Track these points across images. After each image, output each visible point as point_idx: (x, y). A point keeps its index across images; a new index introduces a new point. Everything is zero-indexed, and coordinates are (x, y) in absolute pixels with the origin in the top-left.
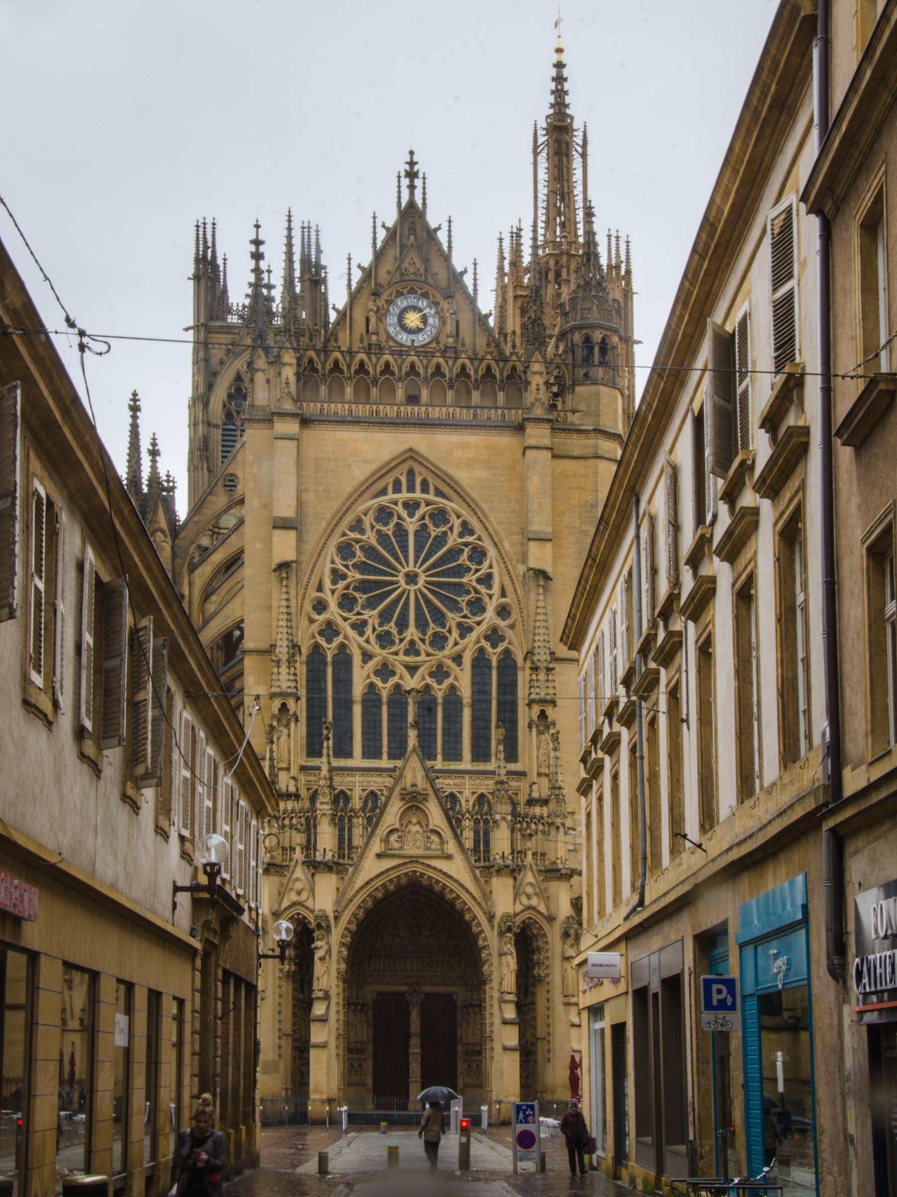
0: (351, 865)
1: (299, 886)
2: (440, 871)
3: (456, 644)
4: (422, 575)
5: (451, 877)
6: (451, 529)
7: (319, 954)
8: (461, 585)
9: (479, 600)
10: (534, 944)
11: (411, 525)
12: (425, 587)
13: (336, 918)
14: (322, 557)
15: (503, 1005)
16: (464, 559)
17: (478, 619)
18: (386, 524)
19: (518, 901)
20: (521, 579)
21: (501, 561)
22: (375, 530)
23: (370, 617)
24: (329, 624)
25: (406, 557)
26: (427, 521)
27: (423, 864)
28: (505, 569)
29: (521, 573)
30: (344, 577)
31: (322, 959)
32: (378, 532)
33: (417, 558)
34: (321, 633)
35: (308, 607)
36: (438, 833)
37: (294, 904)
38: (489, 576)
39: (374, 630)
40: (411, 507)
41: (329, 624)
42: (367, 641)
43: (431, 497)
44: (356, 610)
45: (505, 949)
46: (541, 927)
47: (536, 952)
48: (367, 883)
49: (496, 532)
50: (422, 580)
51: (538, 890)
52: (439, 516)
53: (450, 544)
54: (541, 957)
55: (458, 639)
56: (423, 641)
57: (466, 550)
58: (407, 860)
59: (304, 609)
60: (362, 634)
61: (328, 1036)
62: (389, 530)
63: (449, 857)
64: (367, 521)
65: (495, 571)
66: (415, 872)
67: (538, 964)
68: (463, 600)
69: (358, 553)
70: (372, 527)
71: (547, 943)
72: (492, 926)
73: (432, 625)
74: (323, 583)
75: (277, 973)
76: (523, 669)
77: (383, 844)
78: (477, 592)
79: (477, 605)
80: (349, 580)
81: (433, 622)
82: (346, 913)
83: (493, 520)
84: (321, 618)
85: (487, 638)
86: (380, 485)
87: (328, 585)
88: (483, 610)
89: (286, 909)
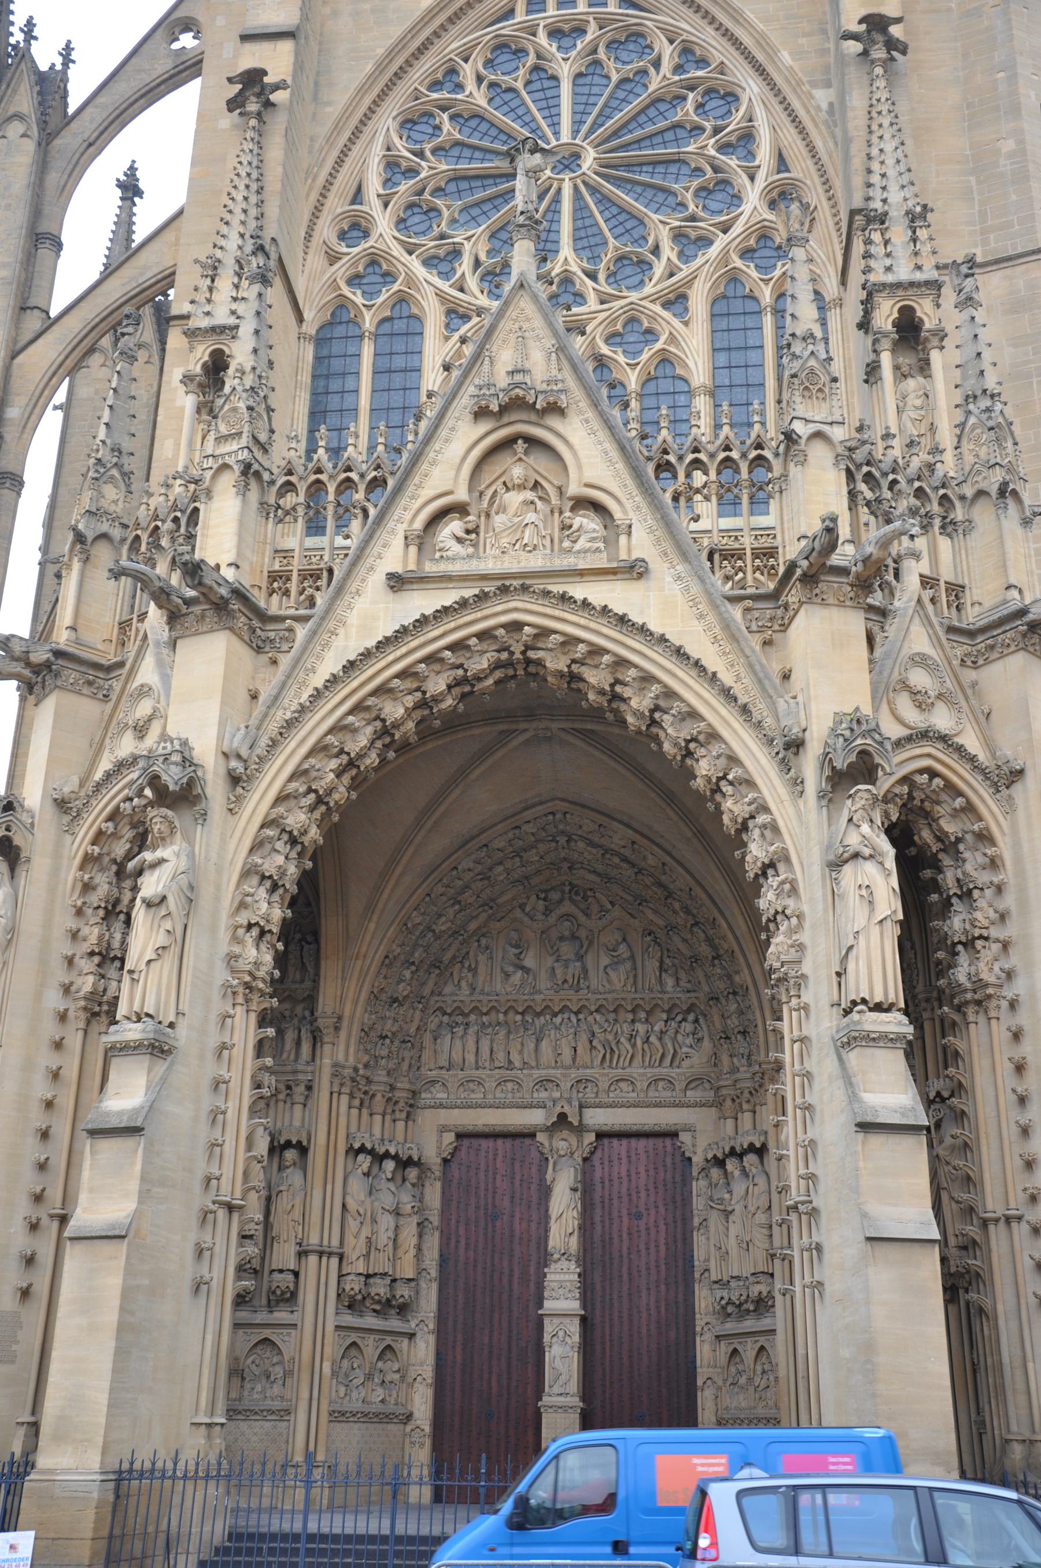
0: (303, 619)
1: (144, 708)
2: (605, 610)
3: (672, 275)
4: (591, 151)
5: (643, 630)
6: (657, 64)
7: (151, 885)
8: (679, 161)
9: (726, 182)
10: (949, 878)
11: (565, 71)
12: (596, 173)
13: (235, 780)
14: (364, 138)
15: (854, 1058)
19: (884, 706)
20: (824, 115)
21: (774, 101)
22: (485, 83)
23: (468, 239)
24: (373, 262)
25: (555, 126)
26: (602, 54)
27: (547, 594)
28: (783, 116)
29: (824, 106)
30: (412, 172)
31: (149, 904)
32: (492, 85)
33: (577, 124)
34: (354, 280)
35: (326, 231)
36: (598, 507)
38: (747, 137)
39: (477, 263)
41: (373, 262)
42: (462, 290)
44: (436, 231)
45: (853, 840)
46: (969, 808)
47: (957, 905)
48: (350, 666)
49: (762, 40)
50: (589, 159)
51: (949, 684)
53: (655, 83)
54: (978, 915)
56: (592, 276)
57: (691, 96)
59: (316, 234)
60: (445, 275)
61: (144, 1196)
64: (468, 72)
66: (516, 626)
67: (969, 944)
68: (686, 190)
69: (447, 126)
70: (480, 79)
71: (994, 864)
72: (797, 783)
74: (364, 189)
75: (54, 1000)
76: (840, 303)
77: (413, 550)
78: (716, 169)
79: (720, 196)
80: (423, 175)
82: (271, 769)
83: (751, 16)
84: (355, 250)
89: (98, 787)
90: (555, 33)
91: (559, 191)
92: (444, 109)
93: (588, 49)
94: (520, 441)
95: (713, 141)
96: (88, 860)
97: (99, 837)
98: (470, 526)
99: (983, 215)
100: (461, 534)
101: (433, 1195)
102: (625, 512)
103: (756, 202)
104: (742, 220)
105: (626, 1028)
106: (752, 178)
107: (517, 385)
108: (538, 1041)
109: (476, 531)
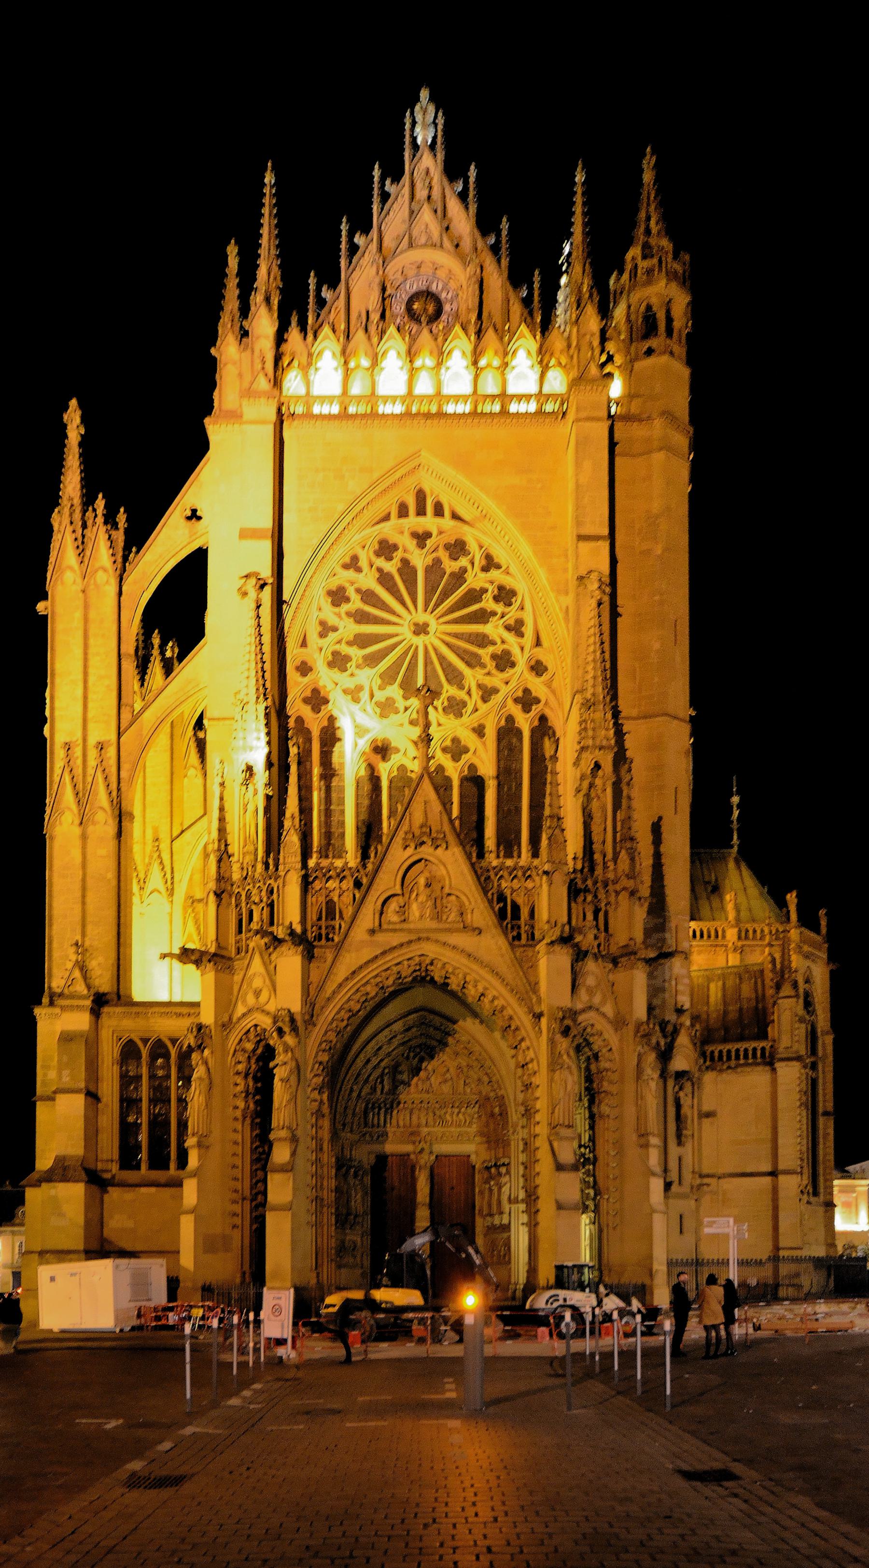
17: (505, 675)
18: (389, 559)
43: (447, 522)
52: (458, 548)
65: (528, 617)
84: (306, 680)
85: (516, 700)
87: (313, 638)
90: (415, 535)
91: (417, 647)
101: (368, 1180)
105: (449, 1110)
106: (522, 649)
108: (411, 1114)
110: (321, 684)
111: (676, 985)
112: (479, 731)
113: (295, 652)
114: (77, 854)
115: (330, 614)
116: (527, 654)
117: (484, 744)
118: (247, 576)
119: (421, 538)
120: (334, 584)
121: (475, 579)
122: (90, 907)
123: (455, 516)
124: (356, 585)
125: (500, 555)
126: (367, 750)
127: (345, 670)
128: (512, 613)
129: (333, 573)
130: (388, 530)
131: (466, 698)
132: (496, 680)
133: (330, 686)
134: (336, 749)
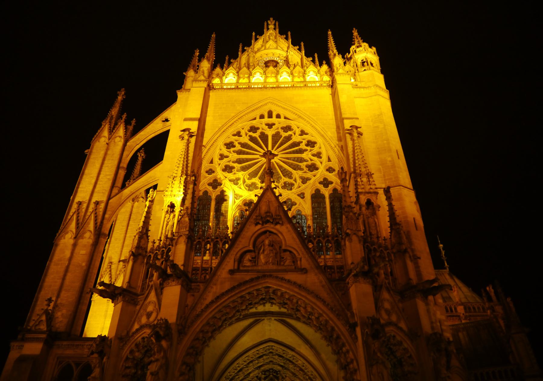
1: (150, 308)
2: (295, 283)
3: (300, 187)
16: (303, 146)
27: (277, 277)
32: (250, 136)
36: (290, 252)
37: (142, 327)
40: (270, 126)
43: (282, 119)
48: (218, 298)
55: (301, 183)
58: (260, 275)
62: (256, 135)
63: (304, 271)
64: (243, 133)
73: (283, 177)
78: (311, 160)
81: (284, 176)
84: (210, 176)
86: (252, 115)
88: (317, 169)
90: (267, 125)
92: (236, 141)
93: (276, 128)
94: (268, 232)
95: (310, 153)
96: (127, 358)
97: (132, 352)
98: (254, 256)
99: (384, 176)
100: (250, 259)
102: (299, 254)
103: (323, 169)
104: (319, 173)
106: (321, 163)
107: (268, 216)
109: (255, 258)
110: (218, 177)
111: (441, 325)
112: (302, 195)
113: (206, 165)
114: (68, 254)
115: (225, 151)
116: (324, 164)
117: (304, 201)
118: (184, 131)
119: (270, 126)
120: (228, 141)
121: (296, 138)
122: (67, 282)
123: (285, 118)
124: (239, 141)
125: (307, 129)
126: (241, 204)
127: (231, 172)
128: (316, 150)
129: (228, 137)
130: (255, 123)
131: (294, 182)
132: (309, 175)
133: (222, 178)
134: (224, 204)
